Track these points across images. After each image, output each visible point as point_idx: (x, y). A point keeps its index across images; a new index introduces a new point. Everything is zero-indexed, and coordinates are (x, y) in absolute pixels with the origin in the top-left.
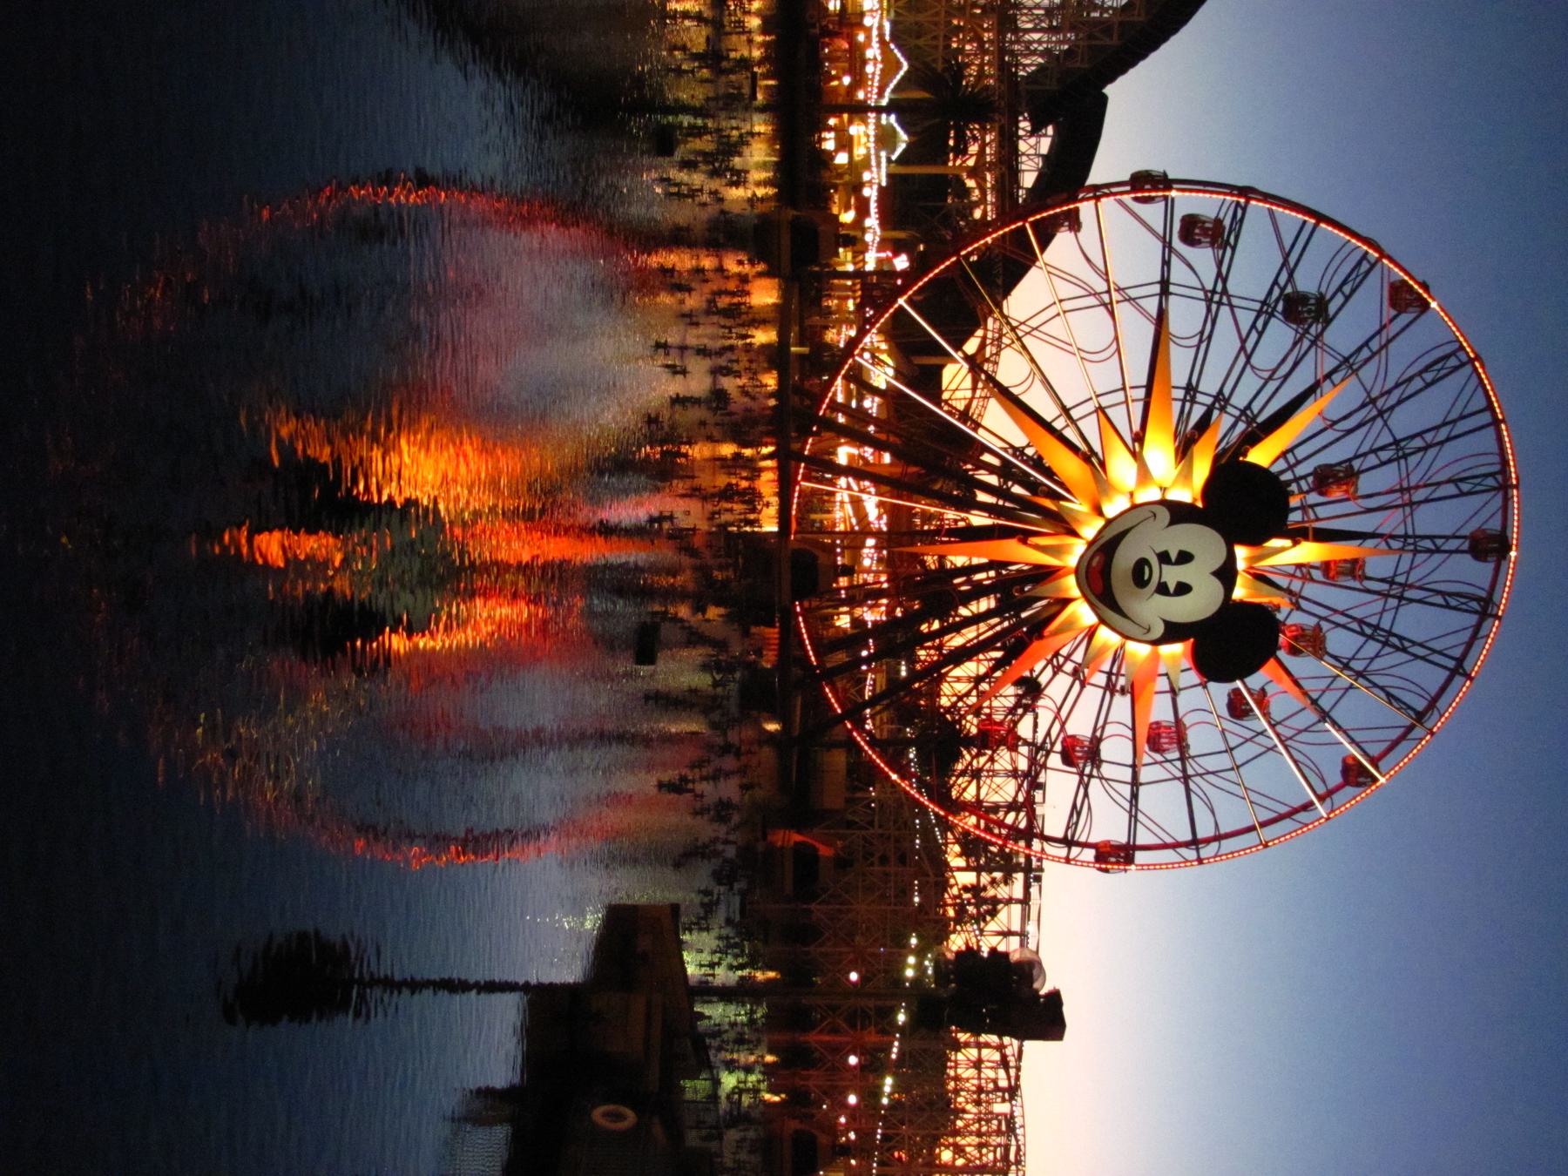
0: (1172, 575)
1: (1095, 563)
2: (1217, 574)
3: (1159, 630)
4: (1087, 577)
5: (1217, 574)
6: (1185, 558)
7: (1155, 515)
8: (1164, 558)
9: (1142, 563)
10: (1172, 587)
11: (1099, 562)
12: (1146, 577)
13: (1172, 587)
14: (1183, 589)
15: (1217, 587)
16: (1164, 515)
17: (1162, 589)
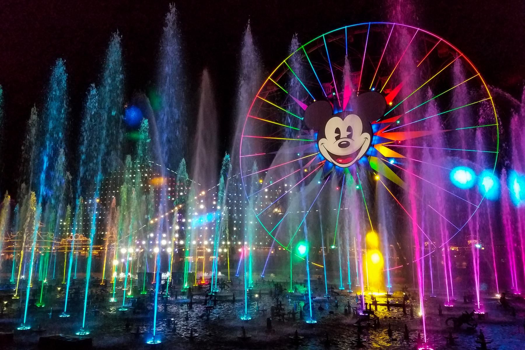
0: (344, 133)
1: (340, 161)
2: (343, 120)
3: (367, 135)
4: (347, 164)
5: (343, 120)
6: (338, 131)
7: (322, 144)
8: (338, 138)
9: (340, 145)
10: (350, 133)
11: (340, 160)
12: (346, 143)
13: (349, 133)
14: (349, 129)
15: (348, 118)
16: (322, 141)
17: (349, 136)
